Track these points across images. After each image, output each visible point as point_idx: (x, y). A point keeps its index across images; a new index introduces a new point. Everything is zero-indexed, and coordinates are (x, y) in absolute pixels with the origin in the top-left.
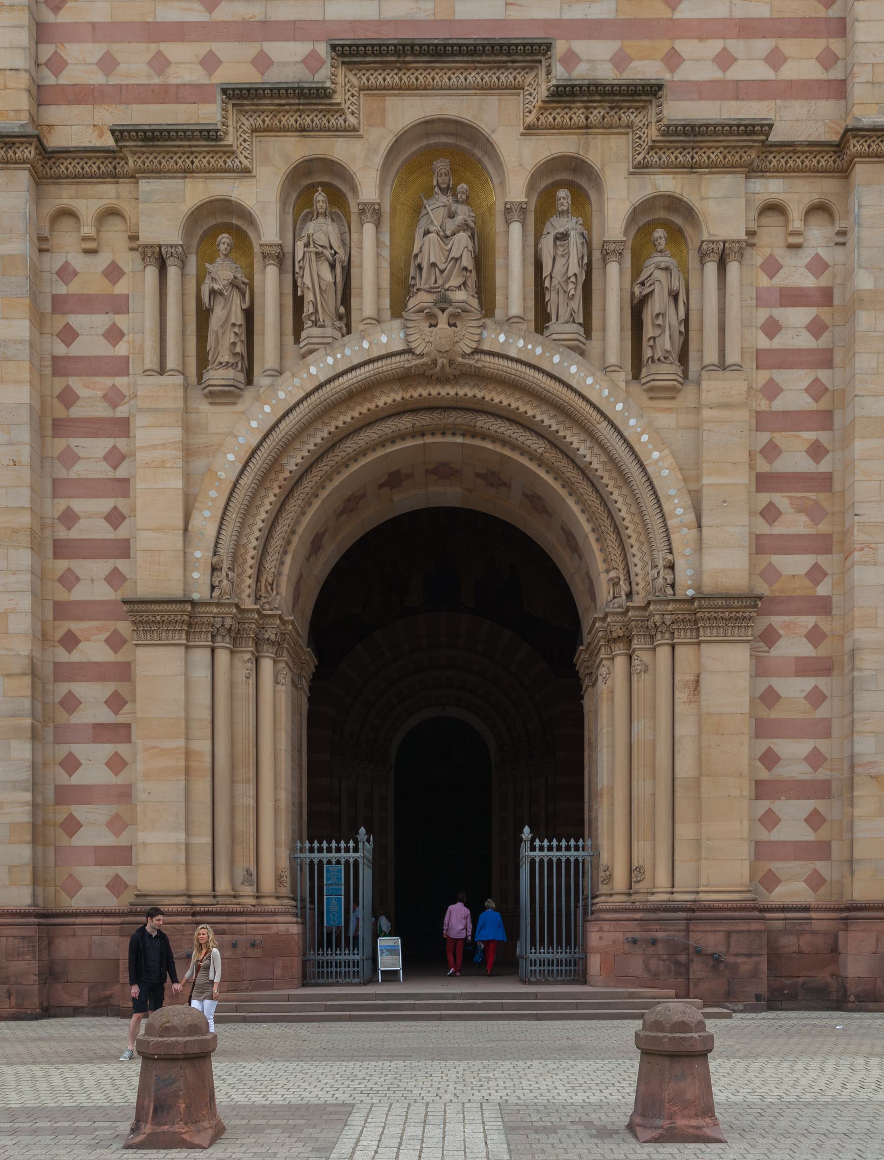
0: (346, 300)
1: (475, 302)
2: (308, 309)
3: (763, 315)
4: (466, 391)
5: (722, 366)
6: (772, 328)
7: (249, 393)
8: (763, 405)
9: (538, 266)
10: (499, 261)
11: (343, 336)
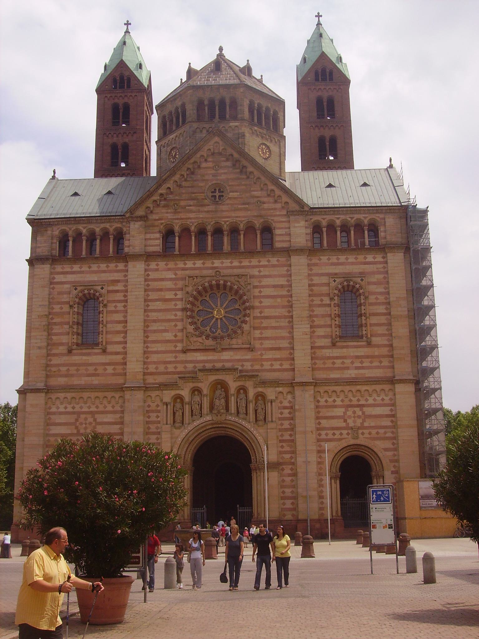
0: (201, 410)
1: (225, 411)
2: (194, 412)
3: (280, 411)
4: (223, 426)
5: (272, 421)
6: (282, 413)
7: (183, 428)
8: (280, 427)
9: (237, 402)
10: (230, 402)
11: (201, 417)
